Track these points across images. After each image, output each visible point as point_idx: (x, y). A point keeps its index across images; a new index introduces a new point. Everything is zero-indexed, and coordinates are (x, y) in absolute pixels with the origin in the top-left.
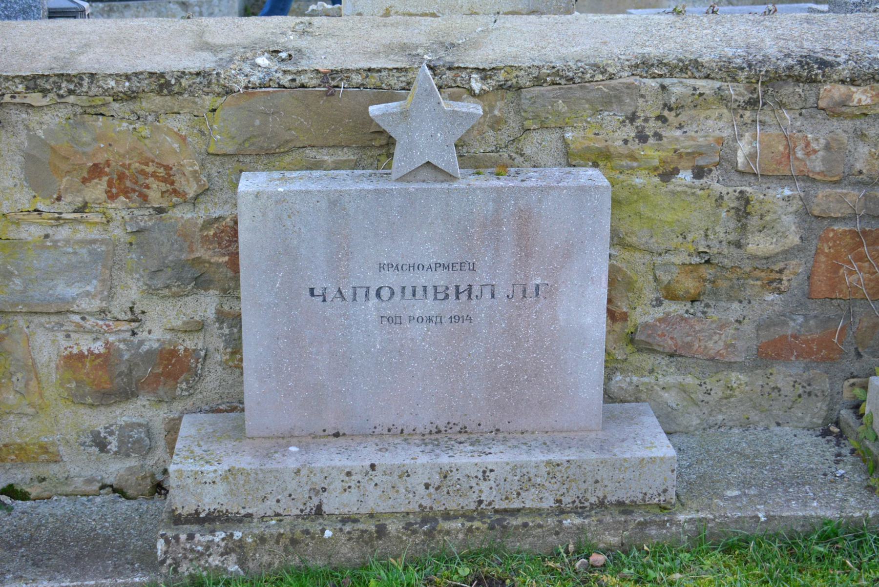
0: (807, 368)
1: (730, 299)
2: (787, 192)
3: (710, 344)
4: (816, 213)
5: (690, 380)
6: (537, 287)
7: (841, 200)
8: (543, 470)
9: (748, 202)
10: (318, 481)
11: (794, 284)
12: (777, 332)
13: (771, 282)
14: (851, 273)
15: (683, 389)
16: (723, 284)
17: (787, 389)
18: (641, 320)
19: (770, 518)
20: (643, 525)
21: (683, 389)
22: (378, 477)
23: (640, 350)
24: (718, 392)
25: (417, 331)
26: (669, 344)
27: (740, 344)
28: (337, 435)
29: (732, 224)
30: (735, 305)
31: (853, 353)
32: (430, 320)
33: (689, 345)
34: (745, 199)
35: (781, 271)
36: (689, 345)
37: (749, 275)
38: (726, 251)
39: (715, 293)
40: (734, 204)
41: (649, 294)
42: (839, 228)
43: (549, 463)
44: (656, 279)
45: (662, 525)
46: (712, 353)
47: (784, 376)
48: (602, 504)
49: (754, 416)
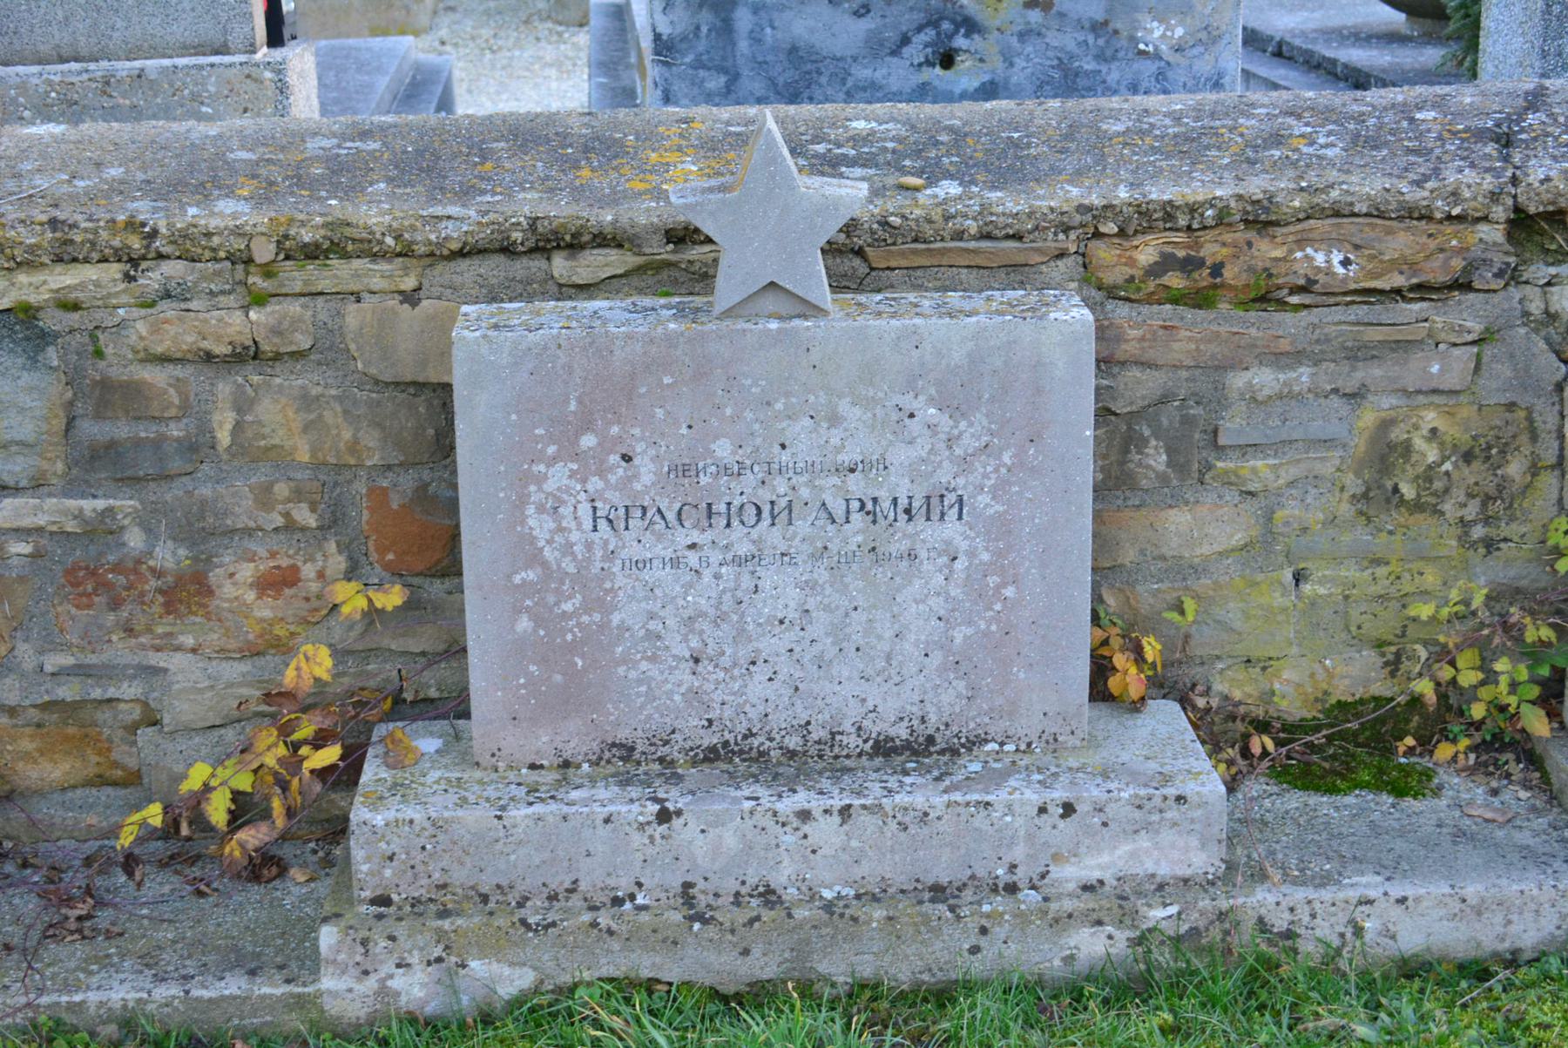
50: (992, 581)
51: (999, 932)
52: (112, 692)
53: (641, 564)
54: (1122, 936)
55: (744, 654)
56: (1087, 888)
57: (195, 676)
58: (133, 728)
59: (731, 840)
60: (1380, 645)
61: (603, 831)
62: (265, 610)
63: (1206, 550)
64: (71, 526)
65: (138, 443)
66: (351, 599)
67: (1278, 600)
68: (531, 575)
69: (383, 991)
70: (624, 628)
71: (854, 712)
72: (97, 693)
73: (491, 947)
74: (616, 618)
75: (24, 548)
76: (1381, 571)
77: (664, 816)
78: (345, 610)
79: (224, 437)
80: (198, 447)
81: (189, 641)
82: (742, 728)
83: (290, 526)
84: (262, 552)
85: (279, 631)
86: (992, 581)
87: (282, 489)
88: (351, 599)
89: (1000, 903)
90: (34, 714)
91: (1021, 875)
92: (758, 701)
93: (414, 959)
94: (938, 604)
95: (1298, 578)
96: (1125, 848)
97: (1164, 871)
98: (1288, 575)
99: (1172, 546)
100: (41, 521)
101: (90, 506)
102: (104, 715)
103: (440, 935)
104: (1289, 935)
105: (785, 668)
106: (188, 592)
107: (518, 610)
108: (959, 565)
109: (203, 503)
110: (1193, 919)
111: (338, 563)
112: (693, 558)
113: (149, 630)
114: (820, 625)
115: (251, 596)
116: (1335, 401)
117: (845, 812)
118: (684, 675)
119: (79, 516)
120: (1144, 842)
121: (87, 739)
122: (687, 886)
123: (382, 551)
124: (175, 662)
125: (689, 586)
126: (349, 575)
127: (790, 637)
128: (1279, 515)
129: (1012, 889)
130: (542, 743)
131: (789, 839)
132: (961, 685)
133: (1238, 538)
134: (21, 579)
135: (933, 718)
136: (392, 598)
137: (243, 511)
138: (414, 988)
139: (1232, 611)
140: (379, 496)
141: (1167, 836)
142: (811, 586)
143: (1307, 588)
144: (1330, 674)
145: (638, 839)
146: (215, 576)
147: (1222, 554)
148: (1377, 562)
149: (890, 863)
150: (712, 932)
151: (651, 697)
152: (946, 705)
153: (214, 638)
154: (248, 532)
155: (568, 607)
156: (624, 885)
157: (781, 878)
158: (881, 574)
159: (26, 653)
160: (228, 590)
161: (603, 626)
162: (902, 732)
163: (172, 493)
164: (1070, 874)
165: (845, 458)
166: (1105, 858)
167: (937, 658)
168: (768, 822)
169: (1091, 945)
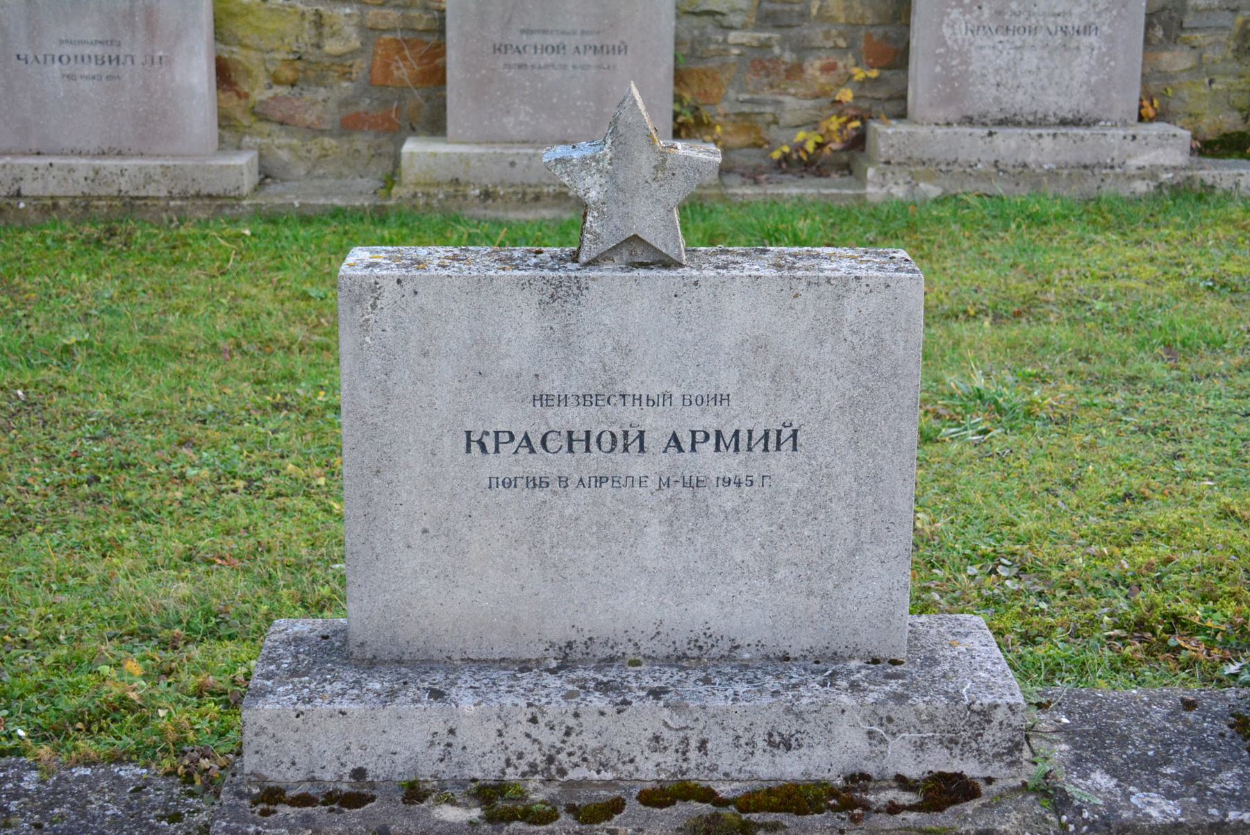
0: (376, 136)
1: (318, 85)
2: (348, 11)
3: (307, 116)
4: (369, 25)
5: (295, 142)
6: (161, 58)
7: (385, 17)
8: (159, 170)
9: (321, 16)
10: (17, 172)
11: (361, 75)
12: (352, 110)
13: (344, 74)
14: (398, 68)
15: (291, 149)
16: (311, 74)
17: (364, 151)
18: (258, 98)
19: (302, 205)
20: (221, 207)
21: (291, 149)
22: (55, 172)
23: (261, 120)
24: (316, 152)
25: (86, 85)
26: (278, 115)
27: (327, 117)
28: (38, 154)
29: (313, 32)
30: (322, 90)
31: (408, 127)
32: (94, 78)
33: (292, 117)
34: (318, 14)
35: (351, 66)
36: (292, 117)
37: (329, 68)
38: (310, 50)
39: (306, 80)
40: (313, 18)
41: (263, 80)
42: (387, 36)
43: (162, 166)
44: (267, 70)
45: (232, 207)
46: (308, 123)
47: (361, 142)
48: (198, 196)
49: (346, 171)
50: (1107, 59)
51: (1108, 181)
52: (762, 110)
53: (981, 48)
54: (1152, 184)
55: (1016, 83)
56: (1139, 168)
57: (794, 105)
58: (769, 124)
59: (1013, 144)
60: (1241, 110)
61: (969, 139)
62: (823, 79)
63: (1175, 69)
64: (755, 43)
65: (783, 12)
66: (859, 74)
67: (1203, 90)
68: (942, 50)
69: (890, 195)
70: (974, 72)
71: (1054, 107)
72: (757, 110)
73: (929, 178)
74: (971, 68)
75: (736, 51)
76: (1243, 80)
77: (990, 134)
78: (856, 78)
79: (814, 11)
80: (804, 15)
81: (792, 91)
82: (1013, 112)
83: (836, 47)
84: (824, 56)
85: (828, 88)
86: (1107, 59)
87: (834, 32)
88: (859, 74)
89: (1108, 171)
90: (733, 117)
91: (1116, 162)
92: (1019, 101)
93: (901, 181)
94: (1086, 67)
95: (1211, 82)
96: (1154, 153)
97: (1167, 163)
98: (1207, 80)
99: (1164, 67)
100: (745, 40)
101: (764, 35)
102: (759, 118)
103: (911, 173)
104: (1213, 187)
105: (1030, 90)
106: (795, 71)
107: (936, 63)
108: (1095, 52)
109: (804, 37)
110: (1178, 179)
111: (852, 61)
112: (1000, 46)
113: (778, 86)
114: (1044, 72)
115: (818, 74)
116: (1227, 12)
117: (1055, 135)
118: (993, 91)
119: (759, 39)
120: (1160, 151)
121: (752, 128)
122: (996, 162)
123: (868, 58)
124: (787, 99)
125: (997, 57)
126: (857, 65)
127: (1032, 78)
128: (1205, 56)
129: (1112, 167)
130: (941, 115)
131: (1034, 144)
132: (1092, 99)
133: (1189, 65)
134: (734, 64)
135: (1082, 111)
136: (874, 74)
137: (819, 40)
138: (899, 192)
139: (1185, 93)
140: (869, 36)
141: (1169, 150)
142: (1042, 58)
143: (1214, 86)
144: (1221, 122)
145: (981, 142)
146: (806, 65)
147: (1184, 71)
148: (1241, 76)
149: (1070, 157)
150: (1006, 176)
151: (981, 99)
152: (1086, 105)
153: (802, 91)
154: (819, 48)
155: (954, 63)
156: (974, 160)
157: (1031, 159)
158: (1067, 55)
159: (732, 94)
160: (810, 71)
161: (966, 71)
162: (1070, 116)
163: (792, 33)
164: (1133, 163)
165: (1057, 11)
166: (1146, 157)
167: (1085, 87)
168: (1026, 137)
169: (1141, 187)
